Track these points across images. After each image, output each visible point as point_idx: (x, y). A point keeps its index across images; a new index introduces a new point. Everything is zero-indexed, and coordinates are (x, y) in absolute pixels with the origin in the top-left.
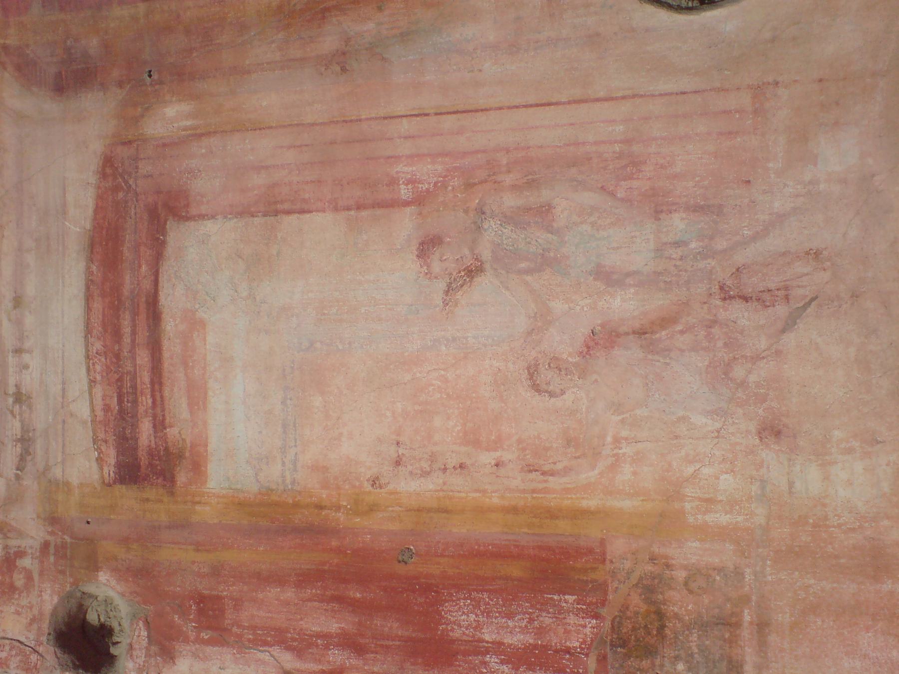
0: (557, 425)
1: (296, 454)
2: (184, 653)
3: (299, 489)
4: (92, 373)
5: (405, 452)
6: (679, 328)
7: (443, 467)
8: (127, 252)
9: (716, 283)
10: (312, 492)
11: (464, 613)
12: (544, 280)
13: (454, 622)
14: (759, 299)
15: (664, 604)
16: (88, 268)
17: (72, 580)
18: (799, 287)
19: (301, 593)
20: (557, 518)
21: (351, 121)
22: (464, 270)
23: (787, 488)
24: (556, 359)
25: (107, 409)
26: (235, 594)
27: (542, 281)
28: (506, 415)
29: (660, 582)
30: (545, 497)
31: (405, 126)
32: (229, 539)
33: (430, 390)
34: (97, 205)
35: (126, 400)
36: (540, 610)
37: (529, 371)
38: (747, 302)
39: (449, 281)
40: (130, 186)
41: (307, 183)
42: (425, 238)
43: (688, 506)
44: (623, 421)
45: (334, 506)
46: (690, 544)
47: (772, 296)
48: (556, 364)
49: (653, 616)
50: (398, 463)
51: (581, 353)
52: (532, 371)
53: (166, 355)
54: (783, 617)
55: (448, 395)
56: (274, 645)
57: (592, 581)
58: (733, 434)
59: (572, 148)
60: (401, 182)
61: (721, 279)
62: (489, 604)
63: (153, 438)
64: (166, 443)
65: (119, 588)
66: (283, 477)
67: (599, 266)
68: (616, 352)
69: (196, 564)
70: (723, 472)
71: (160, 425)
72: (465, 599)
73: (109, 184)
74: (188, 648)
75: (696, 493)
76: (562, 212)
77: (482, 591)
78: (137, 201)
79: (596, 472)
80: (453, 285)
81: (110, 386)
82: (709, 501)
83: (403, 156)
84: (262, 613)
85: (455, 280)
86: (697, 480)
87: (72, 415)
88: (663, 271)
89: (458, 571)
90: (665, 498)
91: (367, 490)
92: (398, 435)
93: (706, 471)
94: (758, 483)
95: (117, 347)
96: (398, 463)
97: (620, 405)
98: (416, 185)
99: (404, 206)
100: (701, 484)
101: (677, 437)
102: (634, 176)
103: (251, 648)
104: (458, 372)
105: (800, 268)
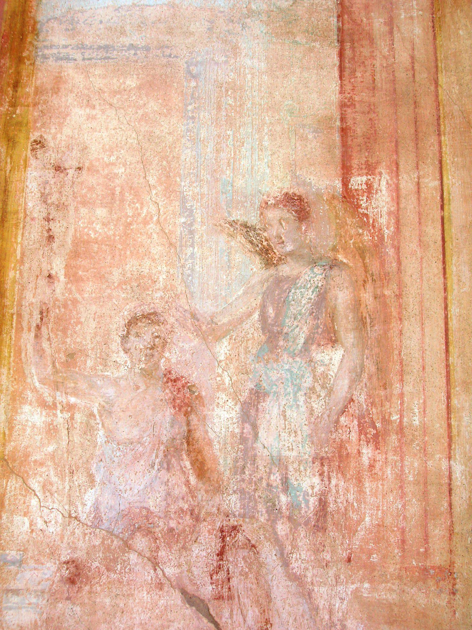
0: (90, 343)
1: (75, 60)
3: (37, 63)
5: (70, 176)
6: (193, 480)
7: (51, 217)
10: (33, 76)
14: (220, 568)
18: (232, 611)
21: (439, 125)
22: (268, 245)
23: (12, 588)
24: (165, 344)
27: (252, 332)
28: (104, 286)
30: (12, 327)
33: (137, 205)
38: (218, 555)
39: (257, 228)
41: (373, 75)
42: (307, 202)
44: (92, 415)
45: (16, 101)
47: (223, 582)
50: (58, 168)
51: (170, 372)
55: (130, 224)
58: (73, 533)
59: (398, 367)
60: (369, 177)
67: (266, 394)
68: (169, 411)
70: (32, 521)
79: (37, 384)
80: (253, 232)
83: (398, 180)
85: (258, 235)
86: (23, 493)
88: (256, 465)
90: (6, 458)
91: (31, 135)
92: (89, 169)
94: (18, 557)
96: (58, 168)
97: (110, 412)
98: (366, 194)
99: (343, 181)
100: (20, 497)
102: (363, 436)
104: (155, 236)
105: (252, 613)
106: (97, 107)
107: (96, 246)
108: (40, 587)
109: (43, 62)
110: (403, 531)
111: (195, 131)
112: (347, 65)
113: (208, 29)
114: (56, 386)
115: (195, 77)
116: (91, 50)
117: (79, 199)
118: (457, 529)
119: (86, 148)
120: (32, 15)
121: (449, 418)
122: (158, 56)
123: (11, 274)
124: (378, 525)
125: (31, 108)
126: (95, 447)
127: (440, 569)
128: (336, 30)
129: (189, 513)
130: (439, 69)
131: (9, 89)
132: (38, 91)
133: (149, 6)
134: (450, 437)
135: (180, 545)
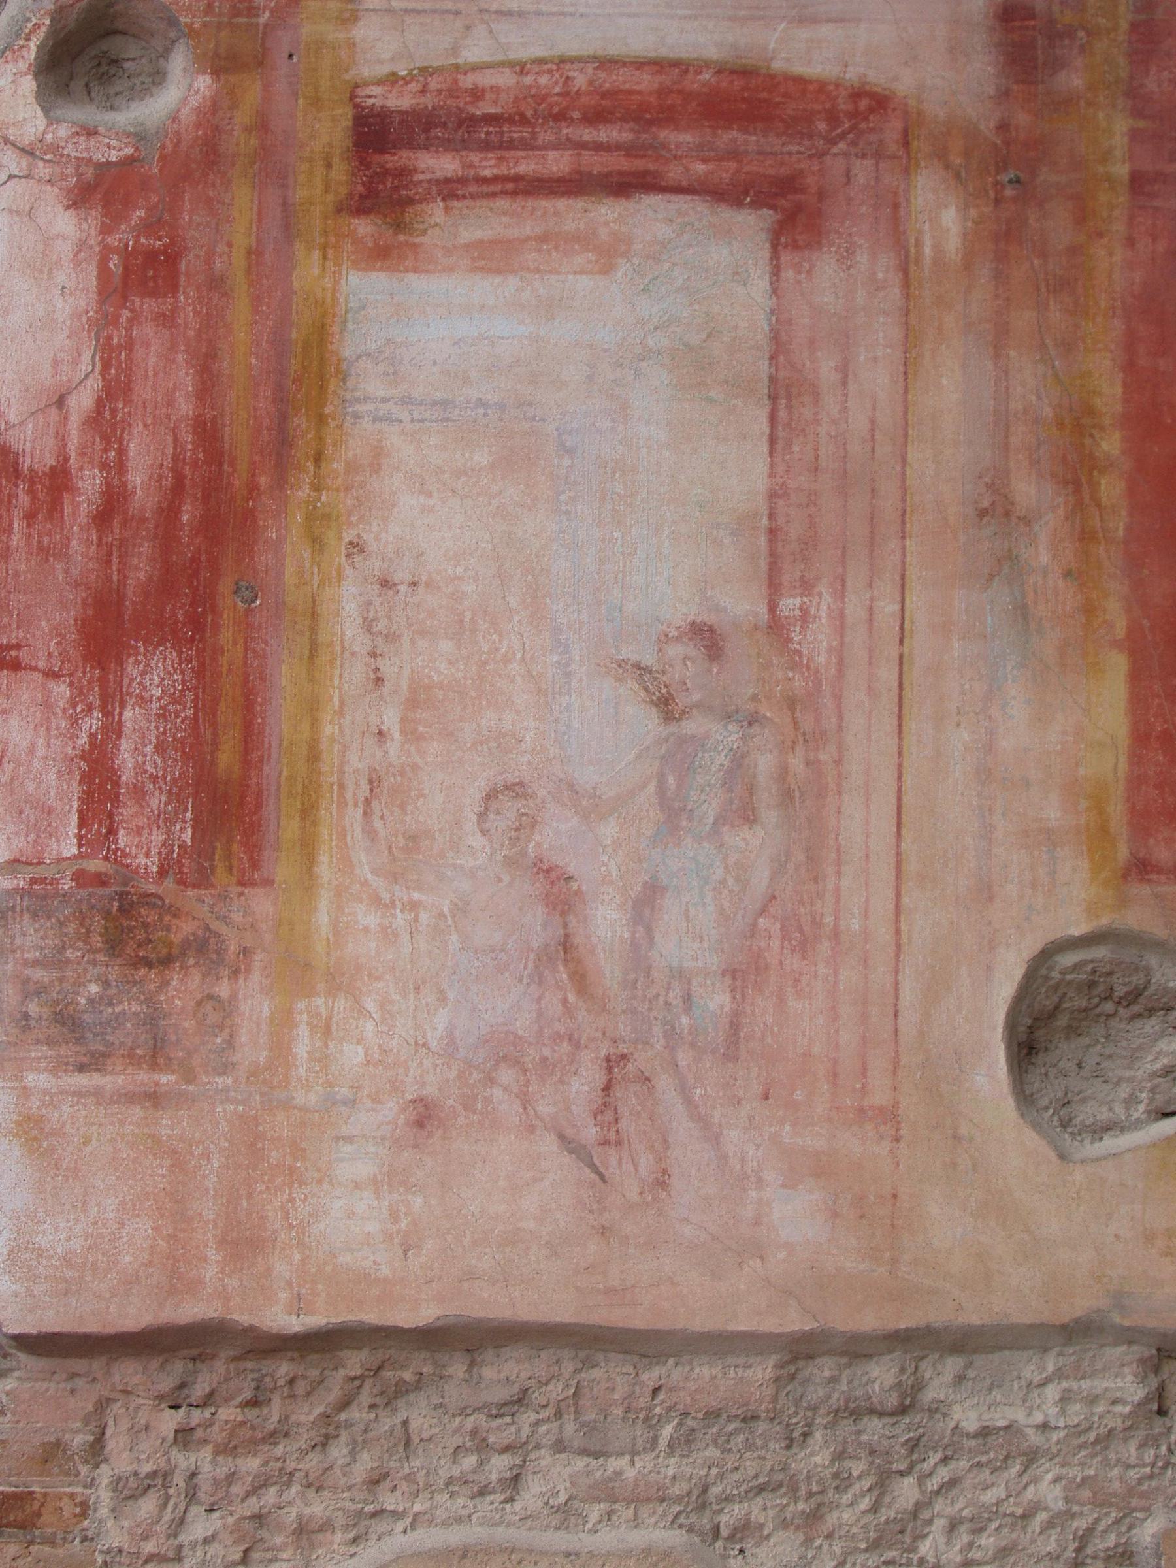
1: (401, 421)
2: (85, 226)
4: (536, 68)
6: (571, 997)
8: (728, 137)
9: (631, 1050)
11: (163, 679)
12: (647, 811)
13: (148, 665)
15: (181, 967)
16: (707, 64)
17: (197, 26)
18: (620, 1159)
19: (187, 425)
20: (303, 819)
21: (904, 523)
22: (669, 693)
25: (477, 94)
26: (182, 316)
28: (454, 748)
29: (214, 962)
31: (888, 608)
32: (268, 308)
34: (810, 82)
35: (491, 129)
36: (170, 792)
37: (518, 784)
38: (603, 1090)
40: (835, 144)
41: (816, 450)
43: (320, 1001)
44: (441, 915)
46: (266, 1003)
48: (526, 825)
49: (165, 951)
50: (385, 583)
51: (541, 860)
52: (517, 789)
53: (561, 204)
54: (167, 1125)
55: (486, 663)
56: (104, 379)
57: (213, 868)
59: (833, 855)
60: (805, 599)
61: (636, 1056)
62: (177, 717)
63: (428, 176)
64: (421, 202)
65: (186, 111)
66: (366, 399)
67: (664, 889)
68: (540, 910)
69: (226, 249)
71: (450, 190)
72: (184, 682)
73: (843, 105)
74: (93, 233)
75: (339, 1013)
76: (744, 839)
77: (196, 707)
78: (810, 157)
79: (369, 876)
81: (514, 102)
82: (327, 1031)
83: (844, 603)
84: (152, 360)
85: (655, 679)
87: (468, 28)
89: (224, 670)
91: (345, 534)
92: (427, 585)
93: (370, 1026)
94: (351, 1096)
95: (576, 115)
96: (385, 583)
101: (417, 988)
103: (98, 341)
104: (519, 679)
105: (646, 1161)
106: (435, 494)
107: (441, 692)
108: (379, 1133)
109: (355, 424)
110: (835, 1062)
111: (571, 532)
112: (781, 434)
113: (588, 377)
114: (394, 877)
115: (569, 452)
116: (422, 408)
117: (415, 627)
118: (904, 1060)
119: (422, 554)
120: (333, 347)
121: (897, 921)
122: (516, 418)
123: (328, 730)
124: (804, 1055)
125: (342, 494)
126: (447, 956)
127: (882, 1110)
128: (766, 379)
129: (567, 1037)
130: (910, 438)
131: (309, 464)
132: (352, 467)
133: (503, 338)
134: (898, 946)
135: (555, 1078)
